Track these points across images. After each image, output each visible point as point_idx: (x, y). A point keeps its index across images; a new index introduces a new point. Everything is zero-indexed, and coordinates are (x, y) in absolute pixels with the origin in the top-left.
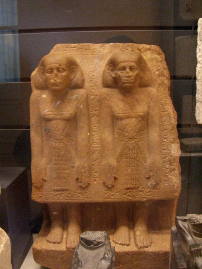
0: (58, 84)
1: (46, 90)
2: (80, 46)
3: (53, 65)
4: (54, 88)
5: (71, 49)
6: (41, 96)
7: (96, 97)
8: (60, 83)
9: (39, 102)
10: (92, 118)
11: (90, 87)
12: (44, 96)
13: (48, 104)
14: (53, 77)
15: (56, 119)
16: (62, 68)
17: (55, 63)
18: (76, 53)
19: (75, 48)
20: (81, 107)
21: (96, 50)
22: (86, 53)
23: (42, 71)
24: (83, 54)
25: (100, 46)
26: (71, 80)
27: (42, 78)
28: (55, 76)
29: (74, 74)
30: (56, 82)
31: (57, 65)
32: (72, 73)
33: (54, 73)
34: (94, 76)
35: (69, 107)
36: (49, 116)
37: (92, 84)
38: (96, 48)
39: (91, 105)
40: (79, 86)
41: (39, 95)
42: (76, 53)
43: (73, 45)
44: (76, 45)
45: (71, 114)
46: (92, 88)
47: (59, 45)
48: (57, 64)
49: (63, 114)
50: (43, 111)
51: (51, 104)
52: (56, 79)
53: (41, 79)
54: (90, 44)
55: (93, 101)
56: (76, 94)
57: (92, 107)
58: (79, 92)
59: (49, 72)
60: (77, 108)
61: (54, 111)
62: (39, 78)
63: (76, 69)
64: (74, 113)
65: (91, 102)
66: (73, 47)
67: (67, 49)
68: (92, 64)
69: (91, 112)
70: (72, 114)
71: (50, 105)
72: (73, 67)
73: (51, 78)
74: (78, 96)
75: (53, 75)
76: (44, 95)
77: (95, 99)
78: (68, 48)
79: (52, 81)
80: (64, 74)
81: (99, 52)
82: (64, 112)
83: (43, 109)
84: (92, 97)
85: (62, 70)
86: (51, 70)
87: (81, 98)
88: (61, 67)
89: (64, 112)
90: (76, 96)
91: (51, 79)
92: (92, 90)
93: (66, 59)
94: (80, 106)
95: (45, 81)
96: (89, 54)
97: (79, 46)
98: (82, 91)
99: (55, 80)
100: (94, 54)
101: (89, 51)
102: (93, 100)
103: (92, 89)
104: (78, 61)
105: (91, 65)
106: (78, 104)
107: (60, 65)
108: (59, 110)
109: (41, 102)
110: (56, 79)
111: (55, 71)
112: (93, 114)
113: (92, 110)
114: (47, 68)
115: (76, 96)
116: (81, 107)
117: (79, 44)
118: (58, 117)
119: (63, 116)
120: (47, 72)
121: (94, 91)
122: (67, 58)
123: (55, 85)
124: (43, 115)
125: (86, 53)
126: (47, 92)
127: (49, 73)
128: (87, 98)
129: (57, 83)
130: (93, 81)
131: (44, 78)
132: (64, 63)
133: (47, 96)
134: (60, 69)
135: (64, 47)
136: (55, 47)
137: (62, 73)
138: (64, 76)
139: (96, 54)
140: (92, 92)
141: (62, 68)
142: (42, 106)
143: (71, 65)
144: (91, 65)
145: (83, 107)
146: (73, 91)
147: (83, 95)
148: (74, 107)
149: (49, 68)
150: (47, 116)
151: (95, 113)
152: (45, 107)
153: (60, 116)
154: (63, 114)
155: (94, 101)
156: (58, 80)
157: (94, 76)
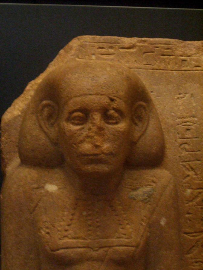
0: (102, 156)
1: (57, 170)
2: (146, 44)
3: (92, 97)
4: (89, 168)
5: (121, 50)
6: (43, 187)
7: (200, 193)
8: (111, 153)
9: (37, 205)
10: (188, 253)
11: (181, 163)
12: (52, 188)
13: (66, 213)
14: (88, 137)
15: (90, 259)
16: (114, 109)
17: (97, 94)
18: (136, 65)
19: (132, 50)
20: (163, 223)
21: (188, 59)
22: (162, 66)
23: (45, 113)
24: (155, 66)
25: (198, 49)
26: (133, 144)
27: (45, 133)
28: (96, 133)
29: (140, 124)
30: (97, 151)
31: (105, 100)
32: (137, 122)
33: (94, 124)
34: (188, 130)
35: (128, 224)
36: (70, 251)
37: (184, 153)
38: (188, 52)
39: (187, 216)
40: (156, 160)
41: (35, 186)
42: (136, 65)
43: (127, 41)
44: (134, 40)
45: (134, 244)
46: (188, 167)
47: (87, 38)
48: (103, 97)
49: (110, 247)
50: (48, 233)
51: (73, 215)
52: (98, 144)
53: (42, 136)
54: (172, 40)
55: (191, 203)
56: (146, 185)
57: (190, 220)
58: (155, 179)
59: (74, 118)
60: (152, 225)
61: (82, 235)
62: (37, 132)
63: (145, 111)
64: (142, 243)
65: (187, 205)
66: (127, 45)
67: (111, 51)
68: (182, 95)
69: (185, 235)
70: (137, 247)
71: (71, 217)
72: (141, 106)
73: (81, 138)
74: (154, 189)
75: (90, 129)
76: (51, 183)
77: (196, 196)
78: (111, 47)
79: (87, 147)
80: (122, 126)
81: (197, 64)
82: (114, 240)
83: (47, 228)
84: (189, 191)
85: (116, 115)
86: (84, 114)
87: (161, 195)
88: (115, 105)
89: (114, 240)
90: (147, 189)
91: (82, 142)
92: (188, 173)
93: (125, 83)
94: (159, 222)
95: (55, 144)
96: (169, 67)
97: (141, 44)
98: (162, 176)
99: (97, 147)
100: (183, 69)
101: (170, 60)
102: (191, 201)
103: (188, 169)
104: (146, 83)
105: (178, 98)
106: (152, 214)
107: (112, 100)
108: (98, 233)
109: (40, 204)
110: (98, 140)
111: (97, 117)
112: (190, 240)
113: (188, 230)
114: (71, 105)
115: (147, 189)
116: (163, 223)
117: (143, 39)
118: (93, 253)
119: (111, 250)
120: (68, 120)
121: (191, 173)
122: (128, 78)
123: (95, 159)
124: (48, 248)
125: (162, 66)
126: (58, 174)
127: (76, 122)
128: (177, 197)
129: (103, 153)
130: (186, 146)
131: (53, 132)
132: (121, 93)
133: (60, 189)
134: (112, 112)
135: (101, 45)
136: (75, 43)
137: (117, 123)
138: (123, 133)
139: (188, 68)
140: (188, 176)
141: (114, 109)
142: (45, 218)
143: (136, 101)
144: (178, 98)
145: (167, 223)
146: (136, 173)
147: (165, 187)
148: (141, 224)
149: (78, 107)
150: (62, 251)
151: (198, 237)
152: (56, 224)
153: (101, 251)
154: (110, 247)
155: (194, 203)
156: (106, 146)
157: (188, 130)
